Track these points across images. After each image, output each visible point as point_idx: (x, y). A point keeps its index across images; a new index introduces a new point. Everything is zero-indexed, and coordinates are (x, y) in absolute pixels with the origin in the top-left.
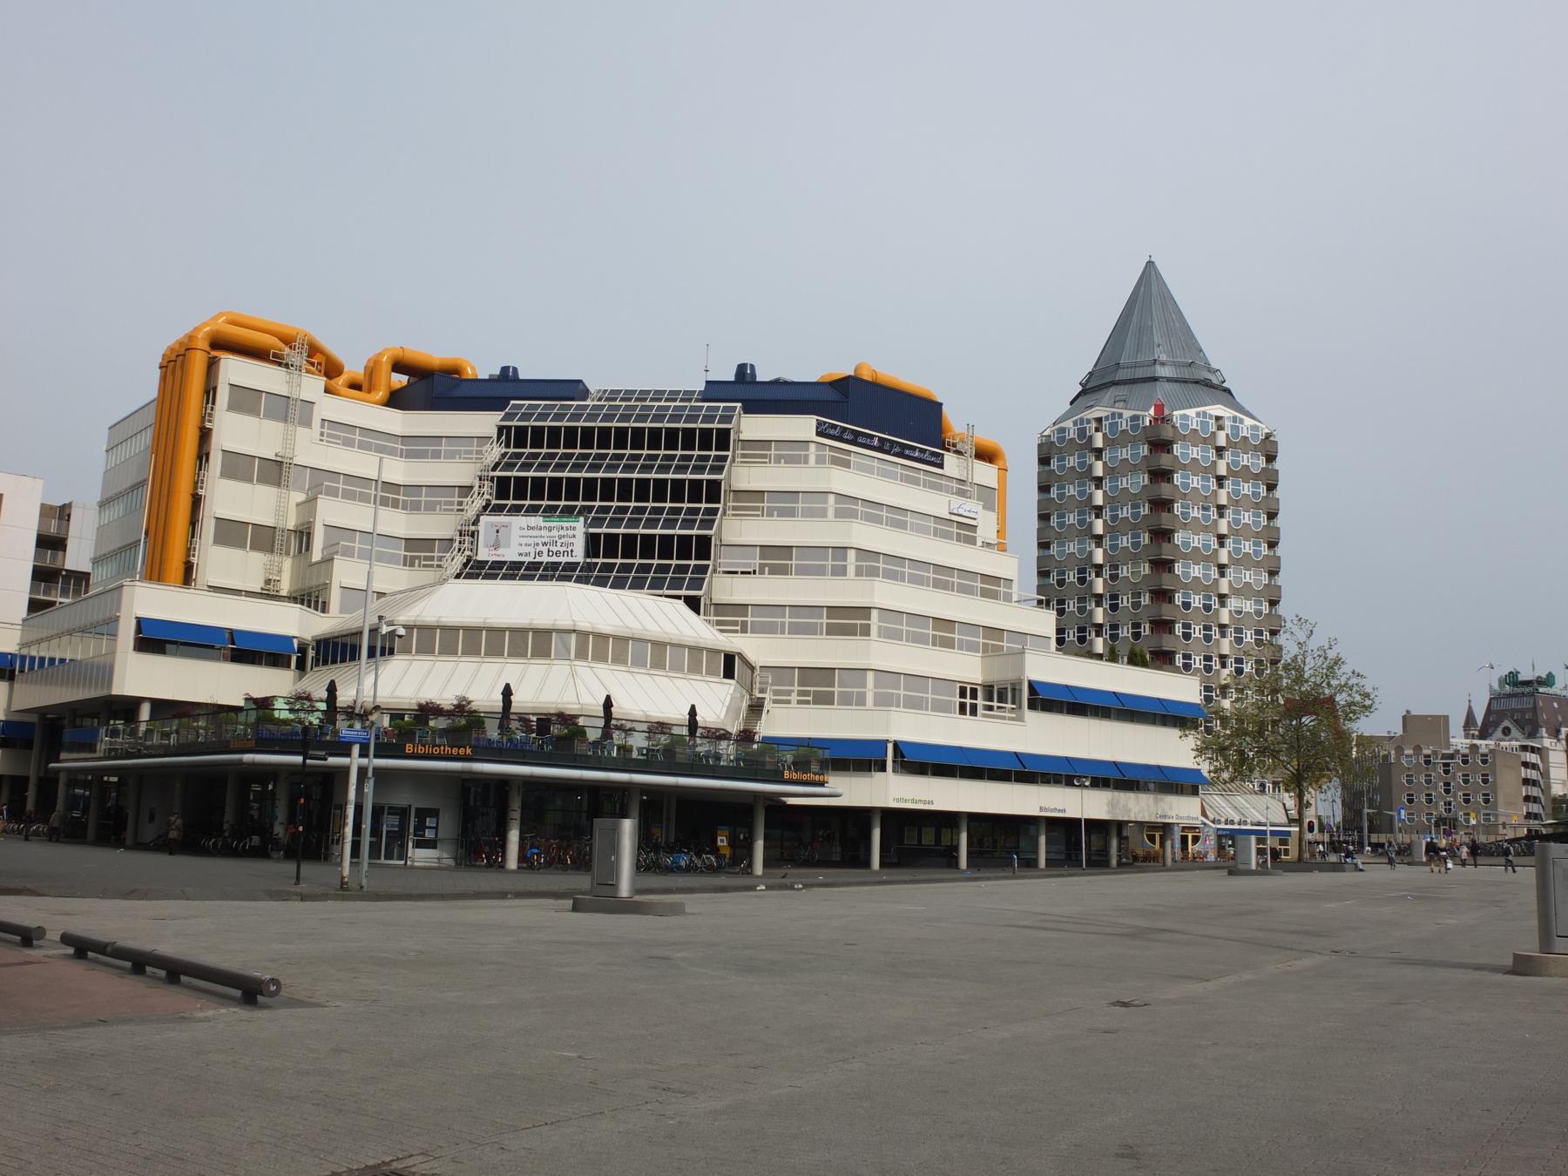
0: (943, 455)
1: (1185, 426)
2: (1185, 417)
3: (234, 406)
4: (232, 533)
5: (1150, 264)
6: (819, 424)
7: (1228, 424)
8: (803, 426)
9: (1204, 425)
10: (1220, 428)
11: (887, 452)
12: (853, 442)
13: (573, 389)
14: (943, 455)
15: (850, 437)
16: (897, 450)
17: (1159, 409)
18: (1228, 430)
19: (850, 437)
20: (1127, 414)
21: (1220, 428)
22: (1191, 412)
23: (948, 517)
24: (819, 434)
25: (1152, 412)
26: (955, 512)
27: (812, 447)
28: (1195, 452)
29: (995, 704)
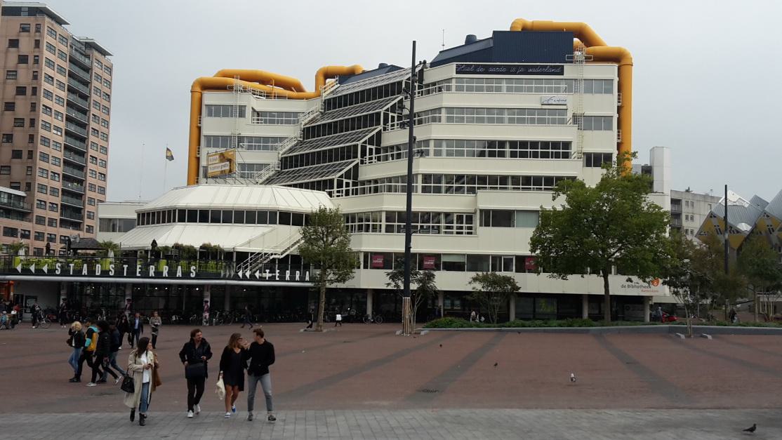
0: (563, 66)
3: (210, 115)
6: (458, 66)
8: (450, 70)
11: (515, 73)
14: (563, 66)
23: (539, 106)
24: (457, 73)
26: (546, 103)
27: (454, 81)
29: (464, 225)
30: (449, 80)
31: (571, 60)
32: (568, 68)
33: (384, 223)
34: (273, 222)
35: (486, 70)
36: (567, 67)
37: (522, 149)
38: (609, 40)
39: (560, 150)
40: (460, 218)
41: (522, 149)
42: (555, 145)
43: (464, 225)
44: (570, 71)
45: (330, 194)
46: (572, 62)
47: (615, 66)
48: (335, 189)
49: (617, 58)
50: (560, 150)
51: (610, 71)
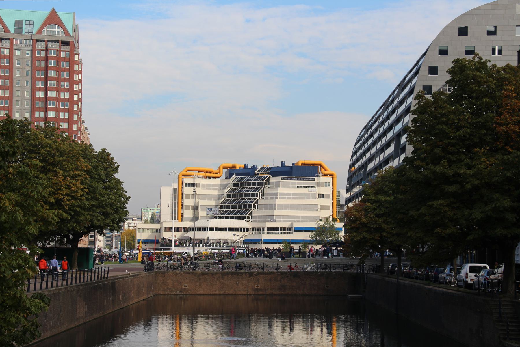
3: (186, 186)
6: (282, 178)
11: (300, 180)
12: (291, 180)
15: (290, 179)
16: (302, 179)
19: (290, 179)
23: (308, 192)
29: (289, 231)
31: (318, 176)
32: (316, 178)
33: (266, 231)
35: (291, 179)
36: (316, 178)
40: (287, 229)
43: (289, 231)
45: (246, 220)
46: (318, 177)
47: (330, 178)
48: (247, 219)
51: (329, 179)
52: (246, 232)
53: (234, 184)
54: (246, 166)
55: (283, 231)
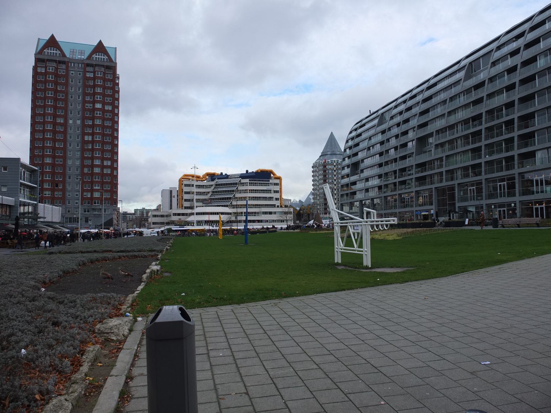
1: (328, 163)
2: (328, 161)
4: (186, 200)
5: (332, 133)
7: (336, 162)
8: (247, 181)
9: (332, 162)
10: (335, 162)
13: (227, 177)
17: (325, 160)
18: (336, 162)
20: (321, 161)
21: (335, 162)
22: (329, 161)
25: (324, 161)
28: (330, 167)
30: (247, 183)
31: (271, 179)
32: (270, 180)
33: (243, 214)
34: (224, 214)
36: (270, 180)
37: (265, 198)
38: (278, 174)
39: (271, 198)
40: (257, 213)
41: (265, 198)
42: (271, 198)
44: (271, 181)
47: (279, 180)
49: (279, 178)
50: (271, 198)
51: (277, 181)
52: (230, 215)
53: (216, 184)
54: (222, 173)
55: (254, 214)
